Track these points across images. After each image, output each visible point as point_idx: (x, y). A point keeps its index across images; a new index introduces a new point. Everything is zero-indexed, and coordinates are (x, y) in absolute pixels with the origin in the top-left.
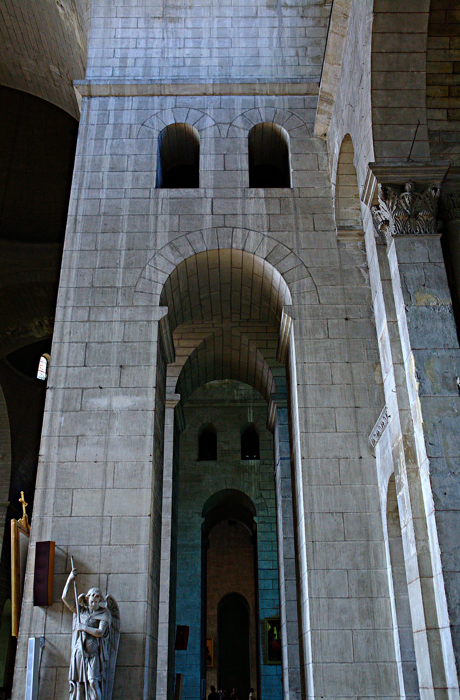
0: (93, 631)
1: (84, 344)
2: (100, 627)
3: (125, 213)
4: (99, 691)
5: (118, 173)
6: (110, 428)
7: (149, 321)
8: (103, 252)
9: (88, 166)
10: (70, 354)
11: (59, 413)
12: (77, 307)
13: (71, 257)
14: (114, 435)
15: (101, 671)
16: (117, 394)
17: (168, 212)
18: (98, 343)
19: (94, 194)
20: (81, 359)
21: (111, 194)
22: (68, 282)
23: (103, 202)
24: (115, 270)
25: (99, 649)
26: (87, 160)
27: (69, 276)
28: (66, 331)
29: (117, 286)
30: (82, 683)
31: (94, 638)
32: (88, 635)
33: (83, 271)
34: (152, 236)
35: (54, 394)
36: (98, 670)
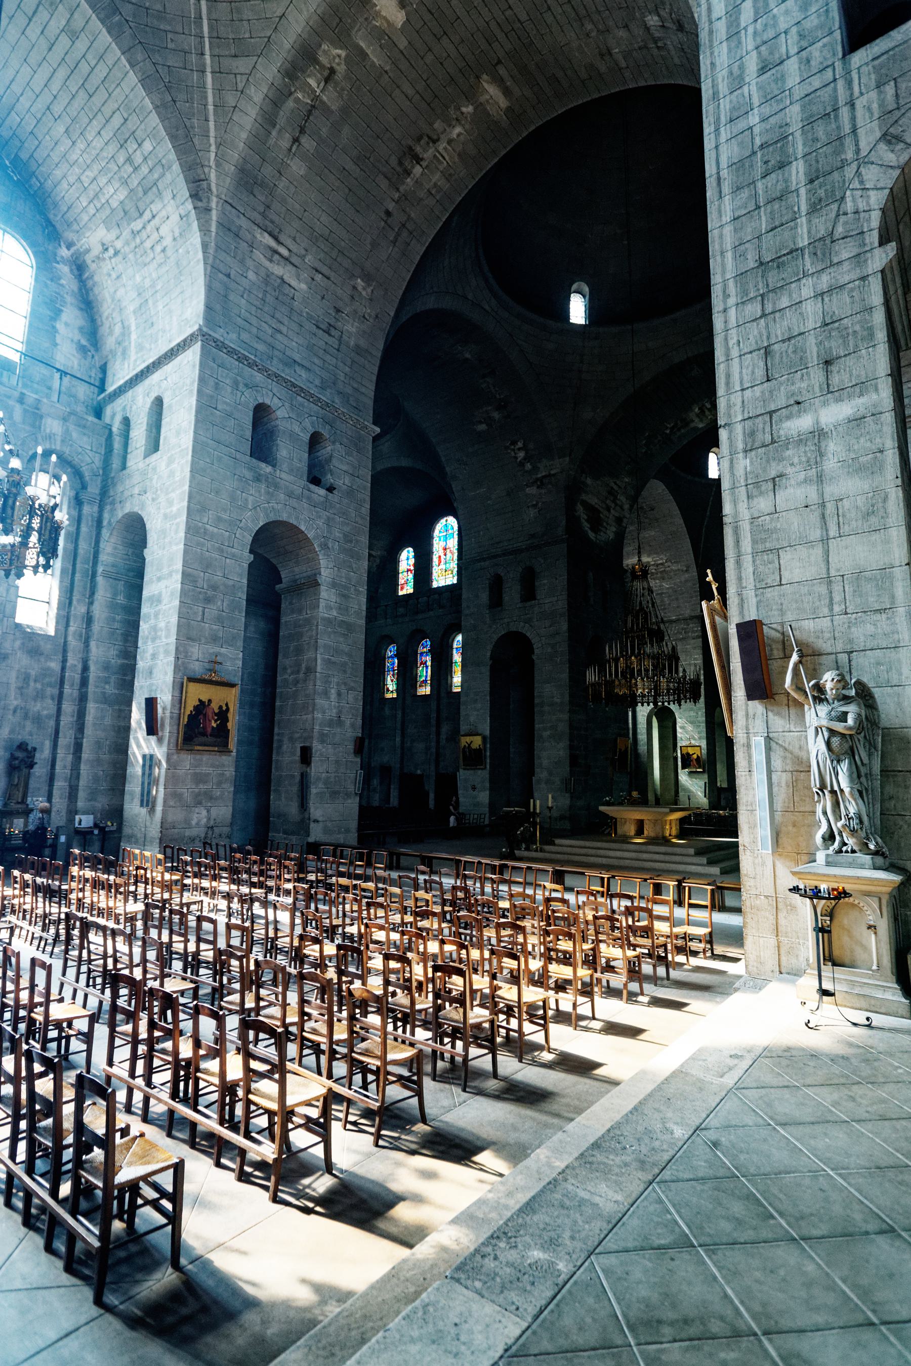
0: (839, 727)
1: (762, 351)
2: (850, 721)
3: (795, 127)
4: (860, 802)
5: (773, 71)
6: (822, 455)
7: (863, 278)
8: (769, 206)
9: (723, 88)
10: (744, 371)
11: (741, 455)
12: (743, 303)
13: (721, 236)
14: (830, 464)
15: (859, 776)
16: (825, 404)
17: (873, 84)
18: (783, 341)
19: (741, 125)
20: (760, 373)
21: (767, 110)
22: (724, 272)
23: (756, 130)
24: (792, 224)
25: (852, 749)
26: (720, 80)
27: (723, 265)
28: (732, 342)
29: (801, 245)
30: (833, 792)
31: (843, 736)
32: (832, 732)
33: (742, 248)
34: (849, 142)
35: (730, 432)
36: (857, 774)
